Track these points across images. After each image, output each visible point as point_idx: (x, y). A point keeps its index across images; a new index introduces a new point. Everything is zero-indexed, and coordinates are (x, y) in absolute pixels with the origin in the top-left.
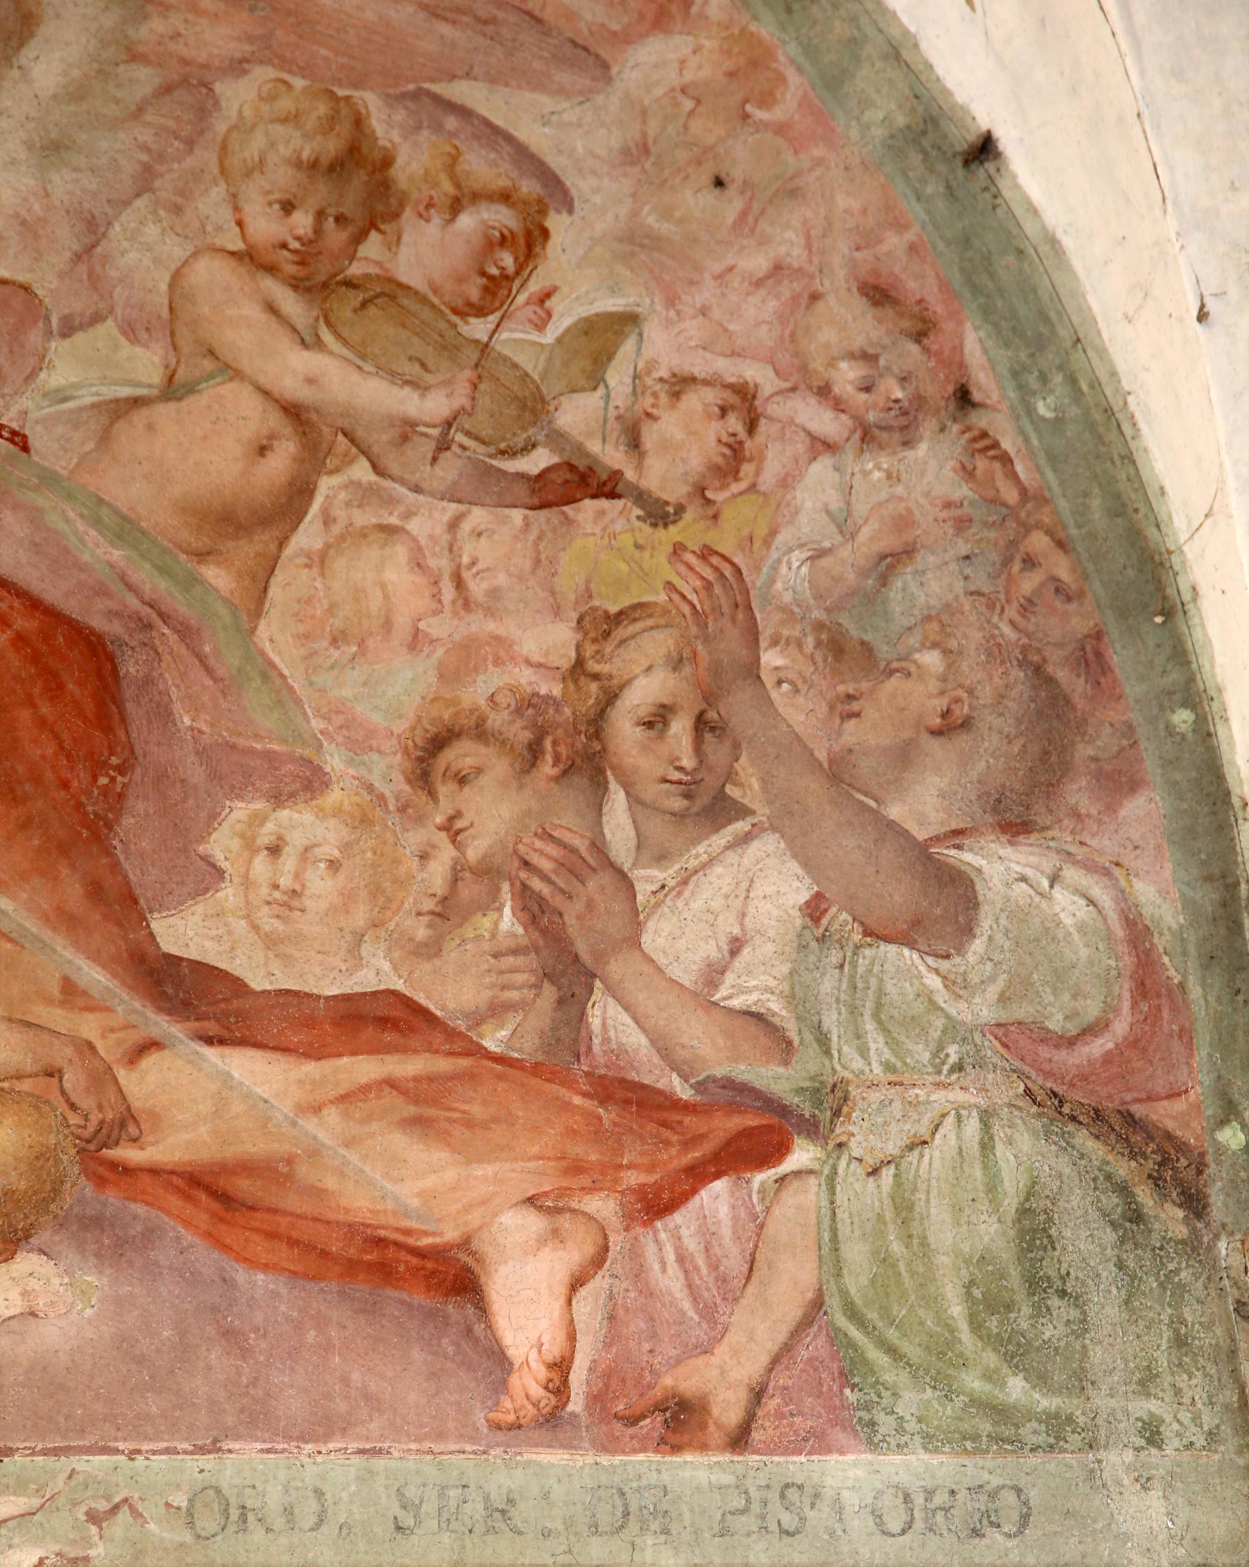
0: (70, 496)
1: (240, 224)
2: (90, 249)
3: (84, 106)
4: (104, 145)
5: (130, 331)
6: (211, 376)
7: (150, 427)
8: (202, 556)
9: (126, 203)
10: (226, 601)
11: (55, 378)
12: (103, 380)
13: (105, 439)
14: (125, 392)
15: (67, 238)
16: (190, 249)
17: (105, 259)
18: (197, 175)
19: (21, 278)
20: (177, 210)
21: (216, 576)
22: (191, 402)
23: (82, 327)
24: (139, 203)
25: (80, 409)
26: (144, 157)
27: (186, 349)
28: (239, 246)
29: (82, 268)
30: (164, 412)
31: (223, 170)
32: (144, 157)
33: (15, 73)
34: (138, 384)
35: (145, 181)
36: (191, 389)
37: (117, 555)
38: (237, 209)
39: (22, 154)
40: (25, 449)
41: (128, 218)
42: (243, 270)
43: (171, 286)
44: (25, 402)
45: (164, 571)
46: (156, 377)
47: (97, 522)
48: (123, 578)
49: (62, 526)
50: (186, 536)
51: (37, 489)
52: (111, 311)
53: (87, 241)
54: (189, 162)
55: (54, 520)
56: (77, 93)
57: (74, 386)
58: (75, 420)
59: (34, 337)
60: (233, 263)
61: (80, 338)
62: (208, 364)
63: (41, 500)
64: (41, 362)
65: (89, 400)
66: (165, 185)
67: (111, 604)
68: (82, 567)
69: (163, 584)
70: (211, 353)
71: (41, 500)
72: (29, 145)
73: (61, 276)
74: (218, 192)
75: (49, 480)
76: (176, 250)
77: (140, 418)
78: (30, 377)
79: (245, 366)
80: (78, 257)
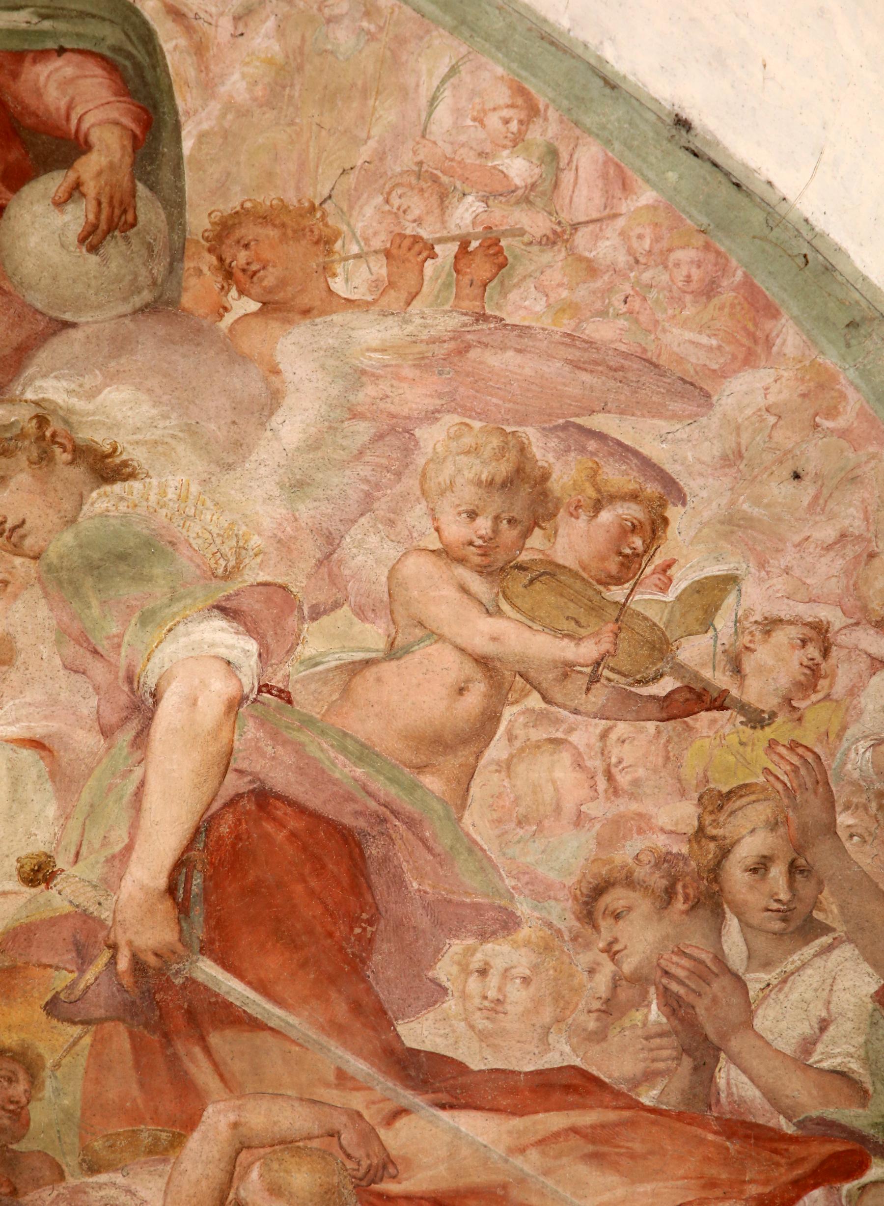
0: (323, 733)
1: (437, 530)
2: (328, 556)
3: (320, 454)
4: (336, 480)
5: (360, 613)
6: (421, 640)
7: (379, 680)
8: (420, 768)
9: (354, 521)
10: (439, 799)
11: (307, 650)
12: (343, 649)
13: (346, 691)
14: (359, 656)
15: (311, 549)
16: (402, 550)
17: (340, 561)
18: (404, 497)
19: (280, 580)
20: (391, 523)
21: (431, 782)
22: (407, 660)
23: (325, 612)
24: (363, 520)
25: (328, 671)
26: (365, 487)
27: (402, 622)
28: (438, 545)
29: (324, 570)
30: (388, 669)
31: (424, 492)
32: (365, 487)
33: (269, 434)
34: (368, 650)
35: (367, 504)
36: (407, 650)
37: (359, 772)
38: (435, 519)
39: (276, 492)
40: (290, 702)
41: (356, 532)
42: (441, 563)
43: (389, 578)
44: (287, 669)
45: (392, 780)
46: (382, 644)
47: (343, 750)
48: (364, 788)
49: (318, 754)
50: (408, 755)
51: (299, 729)
52: (347, 599)
53: (327, 549)
54: (399, 488)
55: (312, 750)
56: (314, 445)
57: (322, 654)
58: (324, 678)
59: (292, 621)
60: (433, 558)
61: (325, 620)
62: (419, 632)
63: (302, 737)
64: (298, 639)
65: (333, 664)
66: (381, 506)
67: (357, 807)
68: (335, 782)
69: (393, 790)
70: (421, 624)
71: (302, 737)
72: (281, 485)
73: (309, 577)
74: (421, 508)
75: (307, 722)
76: (391, 552)
77: (371, 674)
78: (290, 651)
79: (445, 631)
80: (320, 563)
